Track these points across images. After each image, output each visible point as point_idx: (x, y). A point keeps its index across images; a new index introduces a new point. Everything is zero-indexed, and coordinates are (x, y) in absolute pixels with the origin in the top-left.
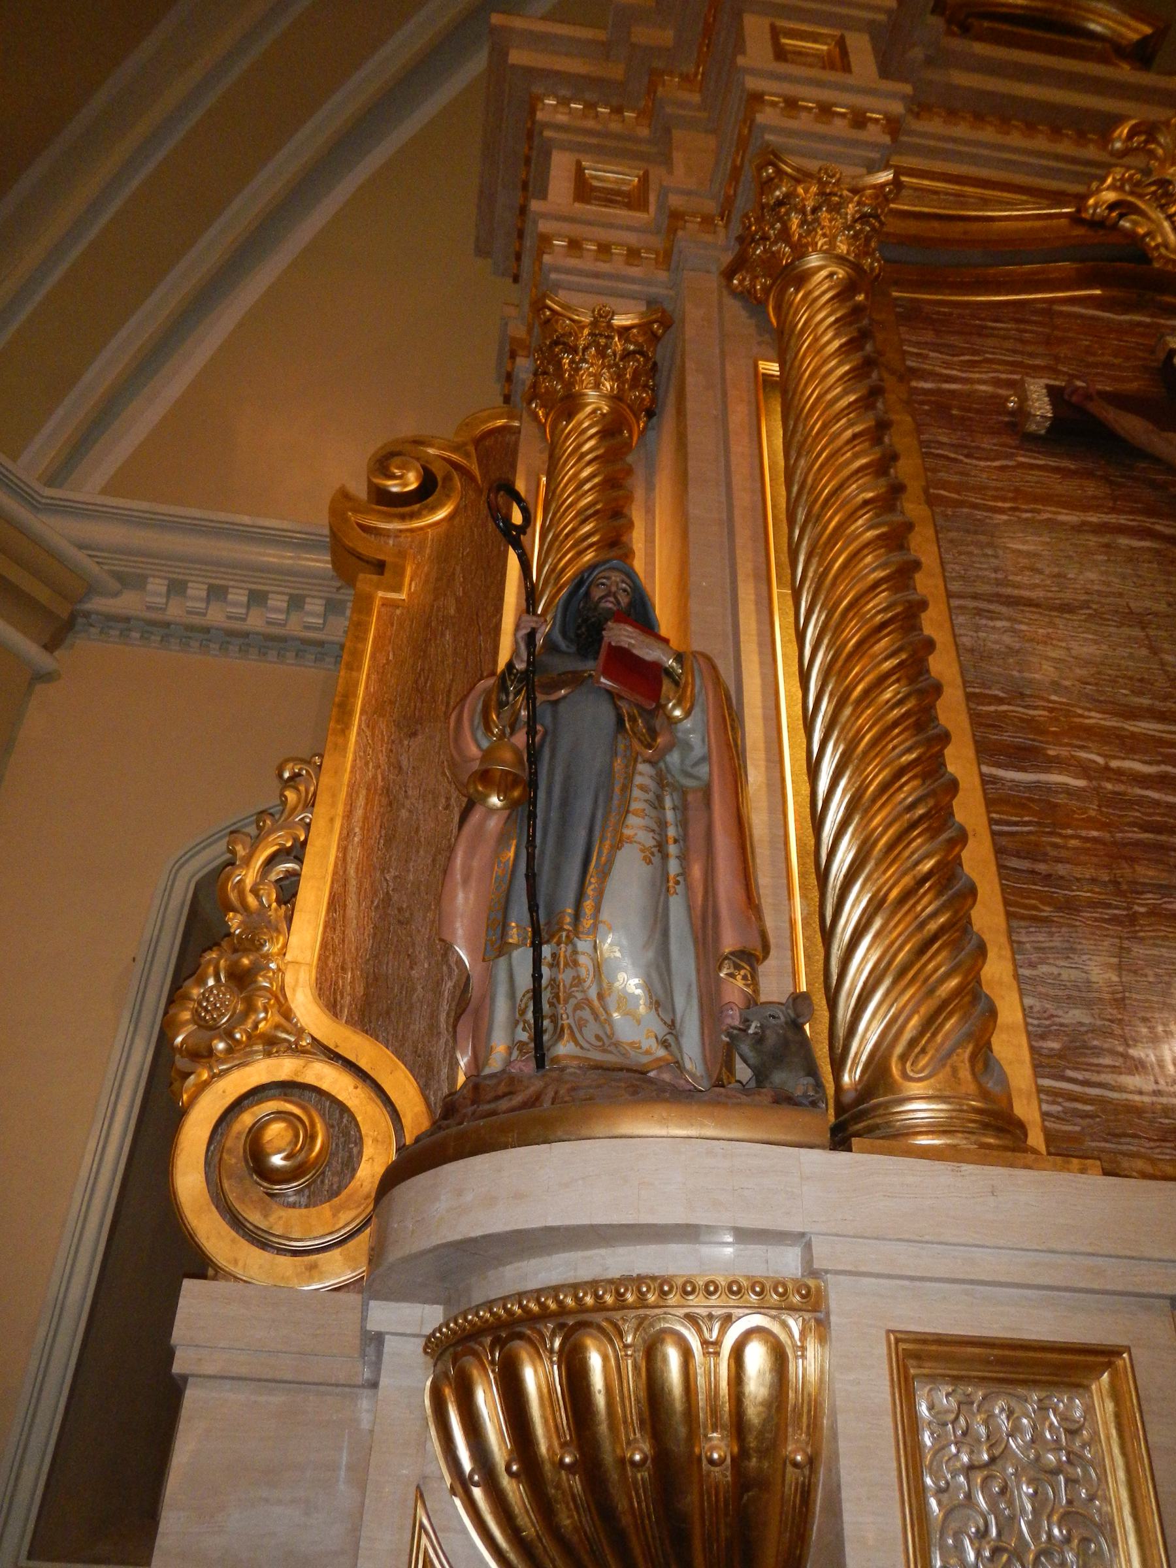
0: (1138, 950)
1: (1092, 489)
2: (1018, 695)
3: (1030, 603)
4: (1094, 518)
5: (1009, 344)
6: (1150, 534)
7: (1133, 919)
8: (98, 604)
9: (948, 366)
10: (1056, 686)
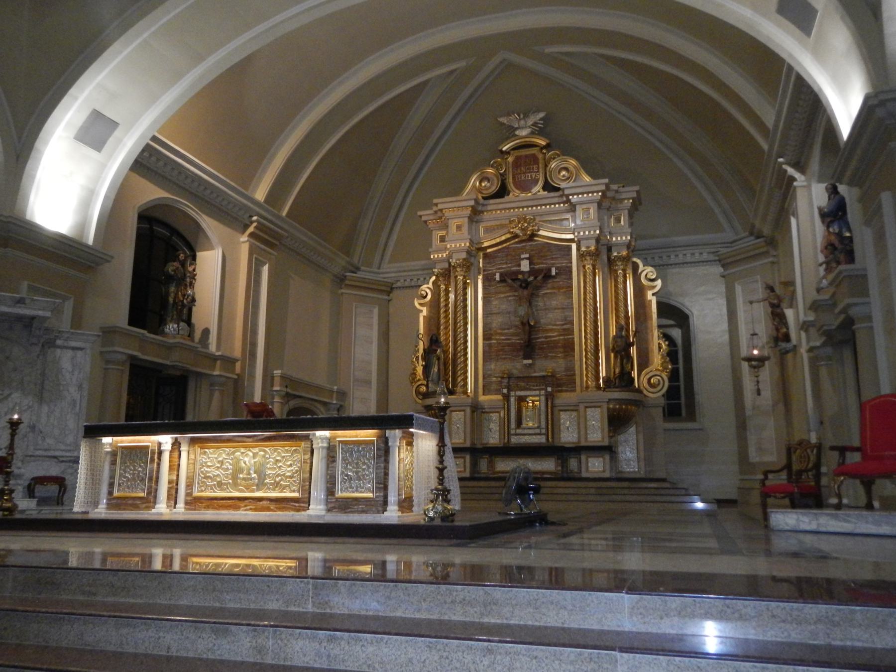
0: (498, 363)
1: (507, 288)
2: (490, 329)
3: (494, 313)
4: (506, 295)
5: (500, 259)
6: (514, 296)
7: (498, 359)
8: (394, 286)
9: (490, 267)
10: (495, 327)
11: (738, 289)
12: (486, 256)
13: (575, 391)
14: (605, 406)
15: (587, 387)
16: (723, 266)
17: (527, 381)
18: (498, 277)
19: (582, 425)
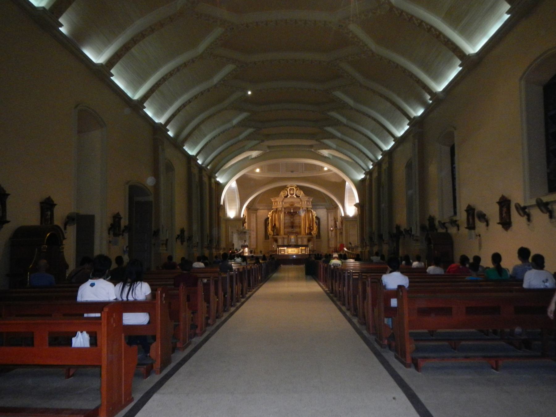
11: (329, 215)
12: (284, 208)
13: (301, 235)
14: (307, 238)
15: (304, 234)
16: (327, 209)
17: (292, 233)
18: (287, 213)
19: (302, 241)
